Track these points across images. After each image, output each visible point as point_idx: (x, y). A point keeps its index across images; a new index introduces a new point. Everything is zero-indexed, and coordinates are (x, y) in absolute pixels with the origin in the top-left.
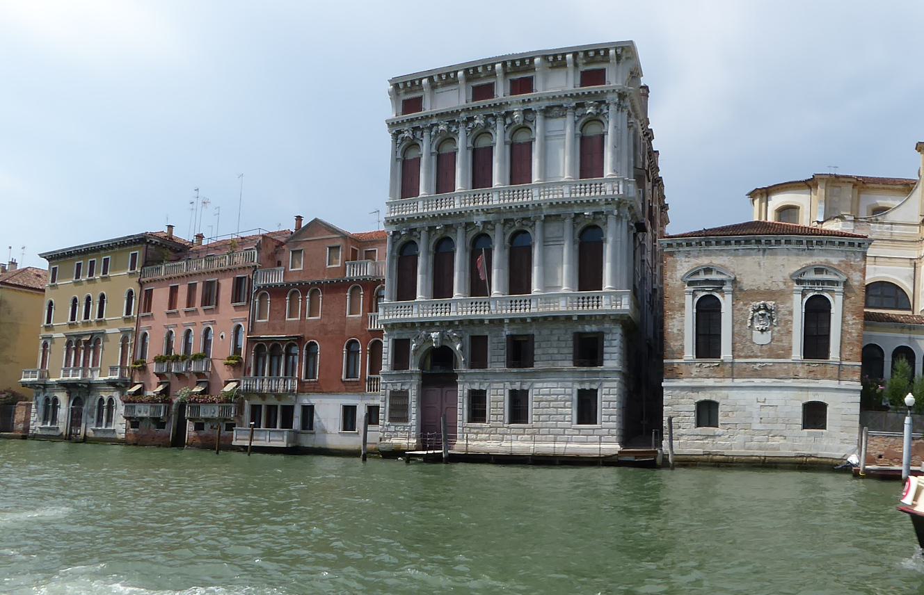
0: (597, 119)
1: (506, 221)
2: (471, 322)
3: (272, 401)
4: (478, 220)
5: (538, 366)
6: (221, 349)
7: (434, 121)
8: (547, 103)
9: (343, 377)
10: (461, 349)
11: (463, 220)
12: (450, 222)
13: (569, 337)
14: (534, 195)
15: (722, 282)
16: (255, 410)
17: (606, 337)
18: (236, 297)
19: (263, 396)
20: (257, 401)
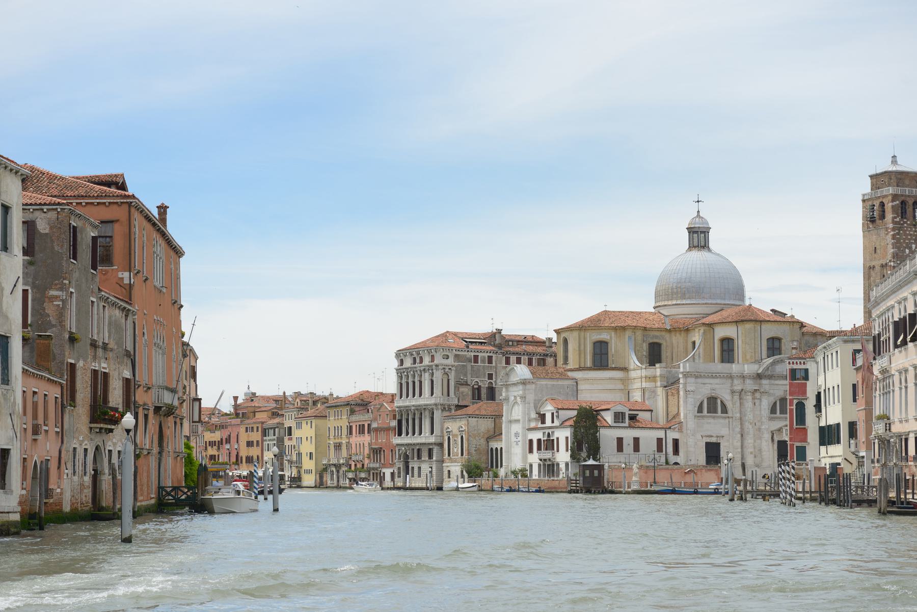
0: (433, 374)
1: (417, 409)
2: (411, 444)
3: (376, 471)
4: (413, 408)
5: (423, 459)
6: (367, 451)
7: (404, 370)
8: (423, 368)
9: (391, 462)
10: (409, 453)
11: (410, 408)
12: (407, 408)
13: (427, 450)
14: (421, 401)
15: (450, 432)
16: (373, 473)
17: (434, 450)
18: (368, 433)
19: (374, 469)
20: (373, 472)
